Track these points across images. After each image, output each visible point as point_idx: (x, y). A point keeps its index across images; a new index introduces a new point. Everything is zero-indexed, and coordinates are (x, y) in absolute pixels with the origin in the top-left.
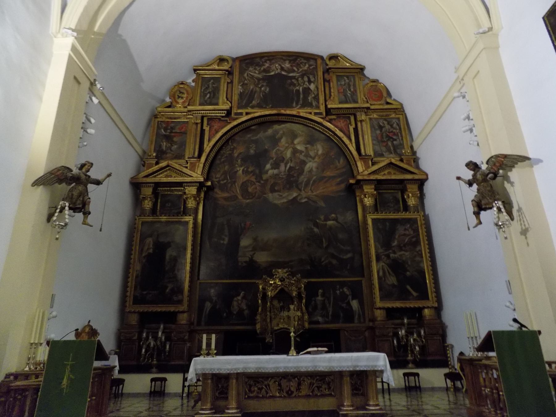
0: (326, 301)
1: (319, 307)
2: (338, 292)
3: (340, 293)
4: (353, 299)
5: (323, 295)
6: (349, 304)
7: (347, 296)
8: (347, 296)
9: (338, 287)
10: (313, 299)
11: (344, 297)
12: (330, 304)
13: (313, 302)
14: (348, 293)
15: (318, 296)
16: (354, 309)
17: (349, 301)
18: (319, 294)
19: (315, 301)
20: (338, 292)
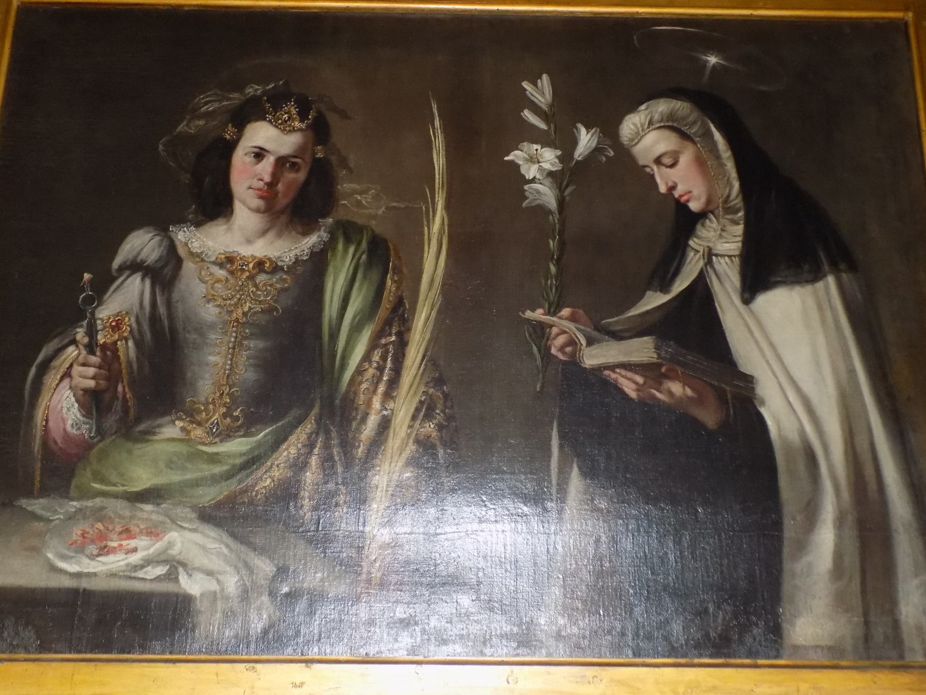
0: (335, 285)
1: (219, 365)
2: (537, 163)
3: (569, 176)
4: (755, 282)
5: (303, 200)
6: (694, 330)
7: (686, 221)
8: (686, 221)
9: (541, 91)
10: (141, 244)
11: (623, 243)
12: (399, 318)
13: (127, 297)
14: (684, 180)
15: (217, 205)
16: (779, 415)
17: (700, 297)
18: (247, 177)
19: (164, 273)
20: (537, 163)
